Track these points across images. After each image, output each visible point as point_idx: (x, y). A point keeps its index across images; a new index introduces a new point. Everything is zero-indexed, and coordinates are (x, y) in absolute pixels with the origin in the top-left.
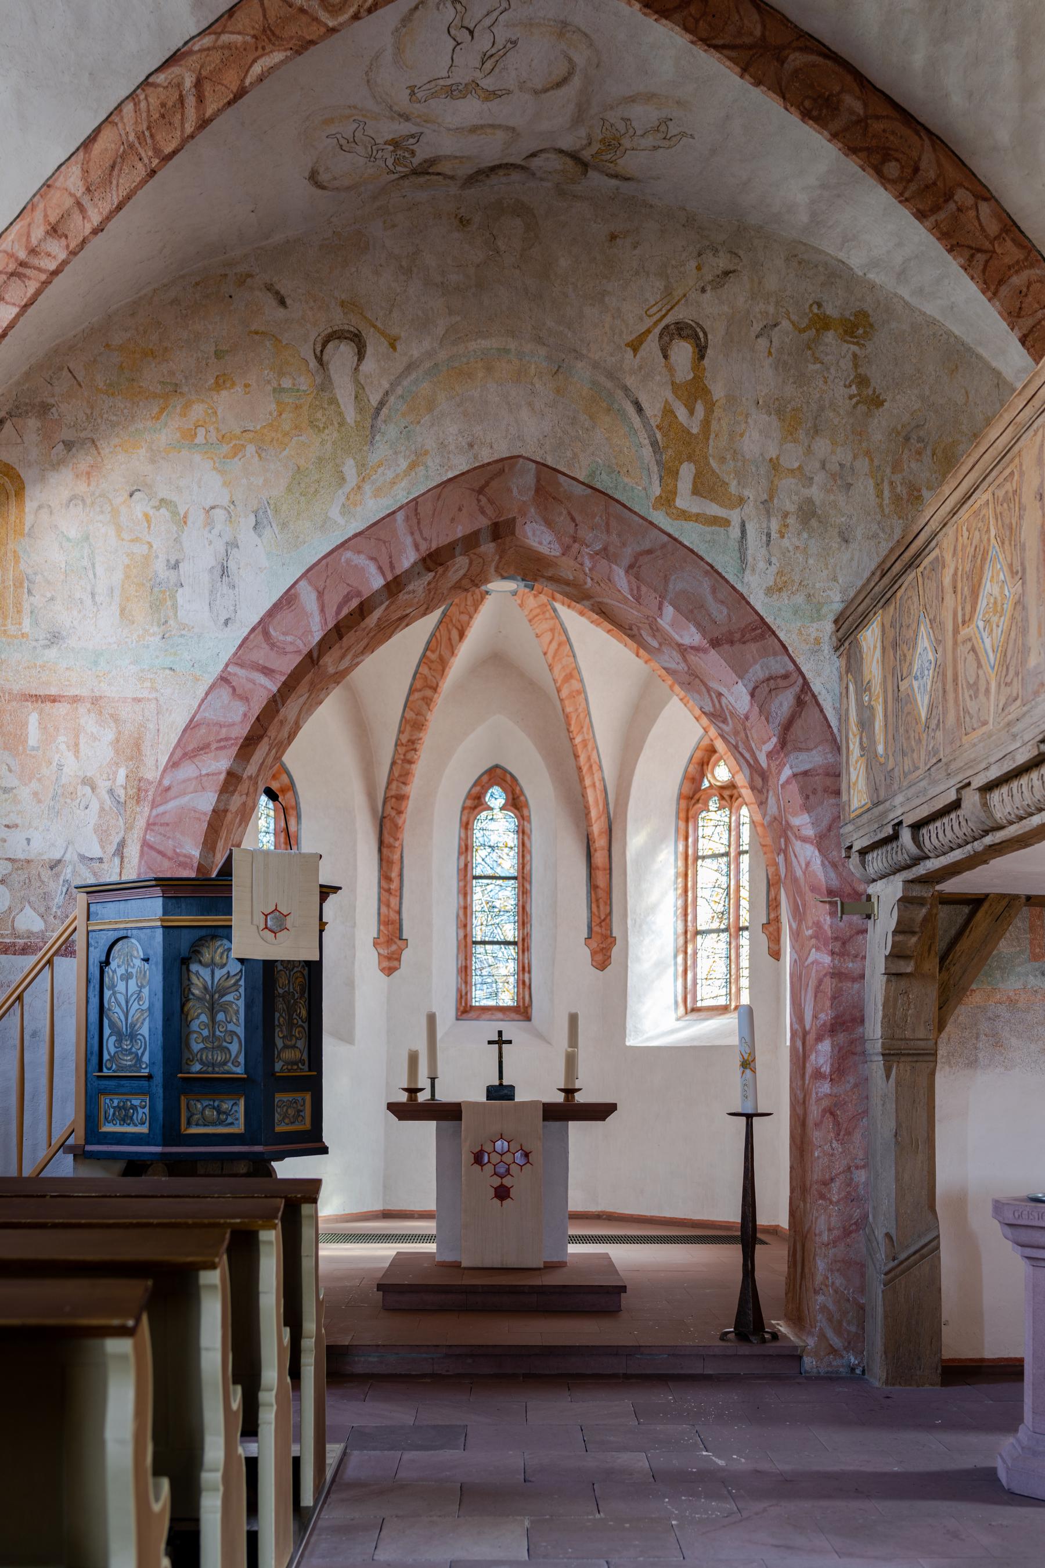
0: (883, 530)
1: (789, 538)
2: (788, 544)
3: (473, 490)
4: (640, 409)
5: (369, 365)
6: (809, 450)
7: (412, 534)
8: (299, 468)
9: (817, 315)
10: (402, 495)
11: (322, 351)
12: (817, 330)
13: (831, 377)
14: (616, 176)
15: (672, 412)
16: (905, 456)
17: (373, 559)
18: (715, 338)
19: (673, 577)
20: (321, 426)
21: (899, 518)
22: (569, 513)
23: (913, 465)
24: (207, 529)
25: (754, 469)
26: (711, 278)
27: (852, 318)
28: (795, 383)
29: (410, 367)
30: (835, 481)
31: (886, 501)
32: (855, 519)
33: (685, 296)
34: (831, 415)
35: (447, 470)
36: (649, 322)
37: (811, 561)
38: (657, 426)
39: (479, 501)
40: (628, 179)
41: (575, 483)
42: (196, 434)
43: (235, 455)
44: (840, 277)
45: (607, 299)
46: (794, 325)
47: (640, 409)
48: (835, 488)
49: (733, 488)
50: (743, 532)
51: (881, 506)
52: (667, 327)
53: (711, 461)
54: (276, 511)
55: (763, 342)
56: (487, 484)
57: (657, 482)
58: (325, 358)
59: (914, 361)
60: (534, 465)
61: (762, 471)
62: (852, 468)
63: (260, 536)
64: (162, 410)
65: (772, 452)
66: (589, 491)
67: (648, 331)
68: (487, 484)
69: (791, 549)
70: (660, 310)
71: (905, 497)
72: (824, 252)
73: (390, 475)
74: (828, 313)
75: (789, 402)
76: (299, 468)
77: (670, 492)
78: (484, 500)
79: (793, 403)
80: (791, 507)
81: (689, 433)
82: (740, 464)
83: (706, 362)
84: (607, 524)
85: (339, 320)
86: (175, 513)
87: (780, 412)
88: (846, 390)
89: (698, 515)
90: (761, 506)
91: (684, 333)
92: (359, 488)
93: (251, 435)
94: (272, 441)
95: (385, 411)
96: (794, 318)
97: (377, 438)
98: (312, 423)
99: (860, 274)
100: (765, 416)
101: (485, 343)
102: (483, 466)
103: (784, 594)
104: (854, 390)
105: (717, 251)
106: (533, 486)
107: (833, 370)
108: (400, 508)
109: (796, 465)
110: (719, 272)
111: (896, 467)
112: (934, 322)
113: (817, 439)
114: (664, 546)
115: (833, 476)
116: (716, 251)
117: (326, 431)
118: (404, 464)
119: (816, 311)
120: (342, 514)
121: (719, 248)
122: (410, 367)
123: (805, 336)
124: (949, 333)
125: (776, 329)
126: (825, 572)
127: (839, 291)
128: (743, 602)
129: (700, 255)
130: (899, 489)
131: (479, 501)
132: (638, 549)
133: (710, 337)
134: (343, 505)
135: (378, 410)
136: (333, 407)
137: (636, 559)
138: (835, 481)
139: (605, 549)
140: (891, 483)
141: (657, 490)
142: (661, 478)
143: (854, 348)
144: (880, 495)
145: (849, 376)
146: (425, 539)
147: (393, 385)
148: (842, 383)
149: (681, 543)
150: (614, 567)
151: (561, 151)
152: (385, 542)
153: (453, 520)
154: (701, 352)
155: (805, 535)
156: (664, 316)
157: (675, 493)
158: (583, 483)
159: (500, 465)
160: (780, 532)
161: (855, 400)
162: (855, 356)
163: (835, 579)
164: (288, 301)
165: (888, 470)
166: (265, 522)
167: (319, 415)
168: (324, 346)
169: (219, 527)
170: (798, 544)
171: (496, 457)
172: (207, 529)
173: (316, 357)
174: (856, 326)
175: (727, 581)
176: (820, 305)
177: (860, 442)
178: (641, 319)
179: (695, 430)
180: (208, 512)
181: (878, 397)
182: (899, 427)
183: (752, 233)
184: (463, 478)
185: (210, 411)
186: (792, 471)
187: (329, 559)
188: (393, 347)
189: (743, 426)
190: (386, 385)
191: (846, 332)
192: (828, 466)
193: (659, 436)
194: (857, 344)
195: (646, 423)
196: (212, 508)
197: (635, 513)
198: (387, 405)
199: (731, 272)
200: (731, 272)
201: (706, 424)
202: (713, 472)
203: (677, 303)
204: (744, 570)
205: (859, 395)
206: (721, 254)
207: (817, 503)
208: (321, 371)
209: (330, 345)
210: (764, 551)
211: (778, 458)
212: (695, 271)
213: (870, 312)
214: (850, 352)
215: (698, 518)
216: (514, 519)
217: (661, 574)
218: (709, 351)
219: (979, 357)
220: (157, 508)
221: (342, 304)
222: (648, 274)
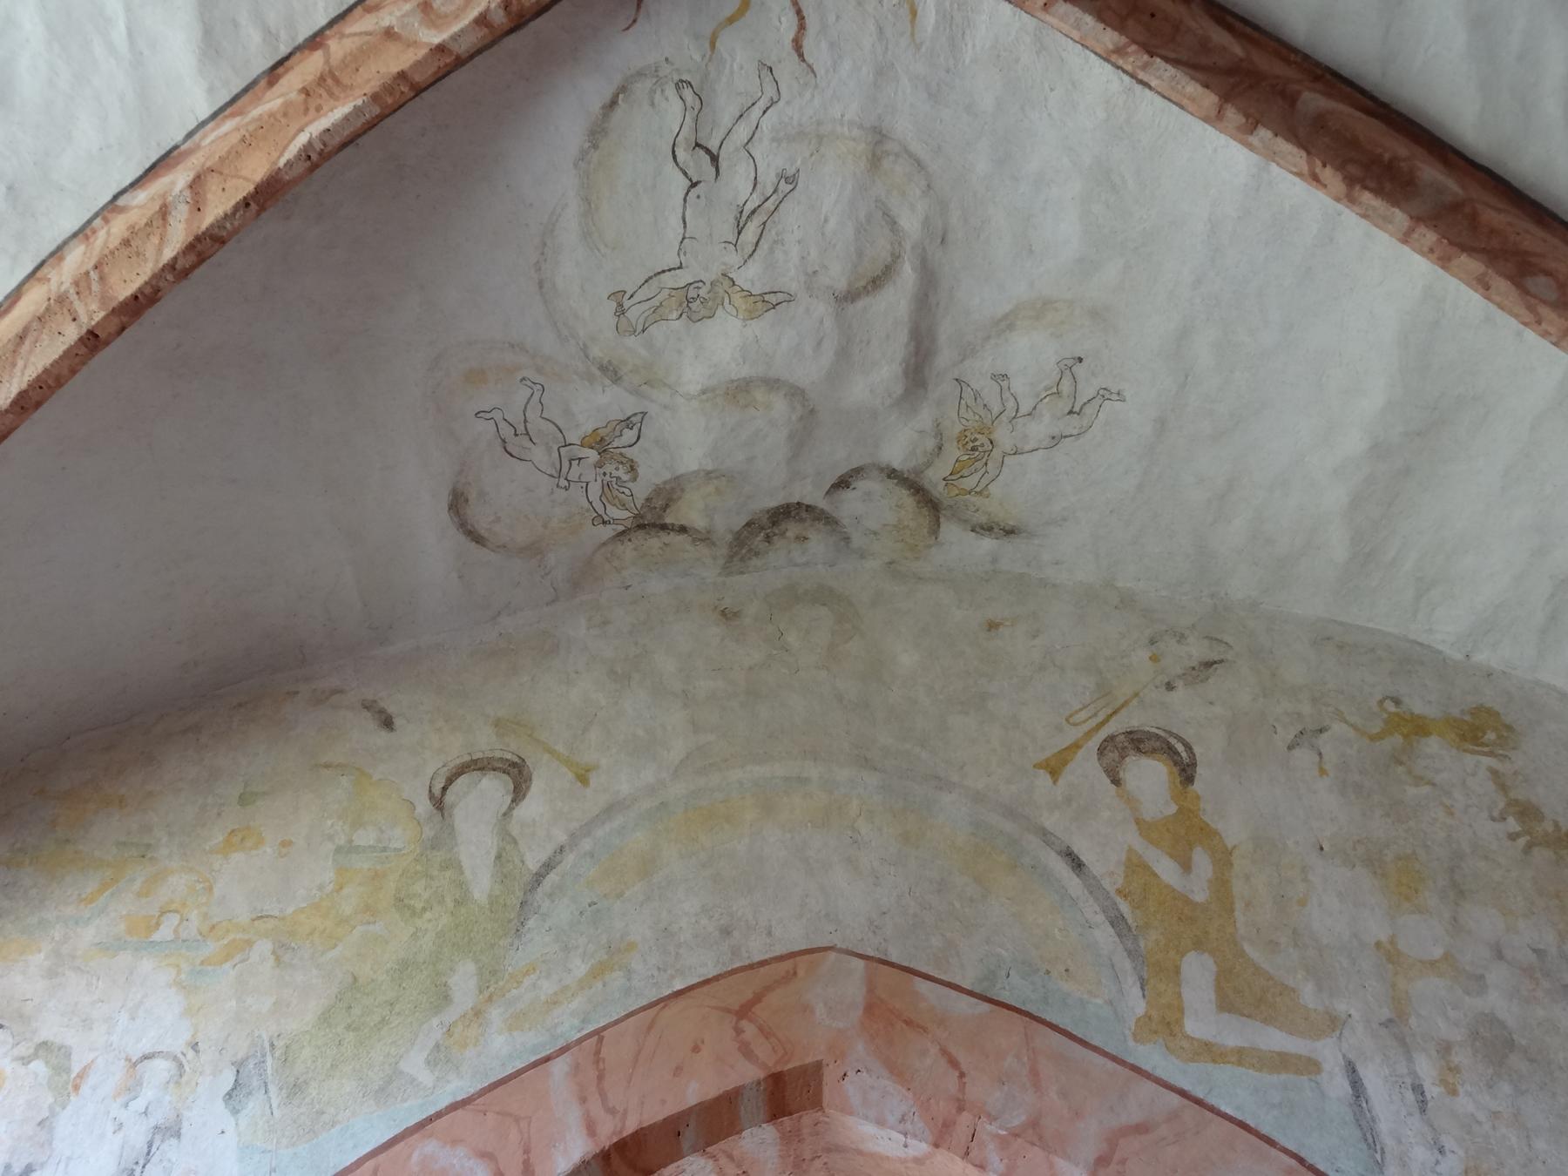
2: (1471, 1108)
3: (728, 1011)
4: (1077, 864)
5: (533, 806)
7: (583, 1100)
8: (355, 979)
10: (568, 1024)
11: (444, 789)
12: (1406, 736)
14: (987, 529)
15: (1146, 867)
17: (486, 1155)
18: (1209, 751)
20: (419, 905)
22: (944, 1052)
24: (121, 1100)
27: (1467, 718)
29: (609, 811)
35: (673, 977)
36: (1072, 735)
37: (1540, 1145)
39: (739, 1031)
40: (1010, 532)
42: (158, 925)
43: (227, 958)
47: (1077, 864)
49: (1308, 994)
50: (1356, 1084)
52: (1111, 739)
53: (1247, 948)
54: (286, 1061)
55: (1303, 756)
56: (758, 999)
57: (1136, 991)
58: (450, 798)
60: (859, 964)
63: (235, 1112)
64: (104, 887)
65: (1377, 930)
66: (985, 1007)
67: (1076, 746)
68: (758, 999)
69: (1481, 1116)
70: (1095, 715)
73: (548, 988)
76: (355, 979)
78: (750, 1029)
81: (1188, 902)
83: (1198, 786)
84: (1034, 1073)
85: (485, 742)
86: (60, 1069)
91: (1147, 746)
92: (477, 1013)
93: (270, 924)
94: (311, 934)
95: (553, 877)
97: (531, 923)
98: (400, 903)
99: (1459, 656)
102: (751, 967)
104: (1513, 824)
105: (1182, 636)
108: (564, 1050)
109: (1438, 953)
110: (1195, 664)
114: (1173, 1116)
116: (1181, 638)
117: (428, 915)
118: (580, 968)
120: (431, 1063)
122: (609, 811)
125: (1325, 736)
134: (437, 1046)
135: (539, 877)
136: (448, 874)
139: (1034, 1123)
141: (1140, 1007)
146: (612, 1111)
147: (574, 838)
150: (1060, 1163)
151: (892, 473)
152: (517, 1120)
153: (678, 1071)
154: (1186, 772)
156: (1103, 723)
157: (1181, 1010)
159: (788, 965)
160: (1444, 1082)
161: (1522, 841)
162: (1494, 773)
164: (398, 722)
166: (255, 1082)
167: (419, 887)
168: (450, 781)
169: (148, 1094)
171: (779, 950)
172: (121, 1100)
173: (431, 796)
179: (1200, 896)
180: (135, 1065)
184: (705, 989)
185: (199, 886)
186: (1433, 964)
187: (381, 1157)
188: (583, 779)
190: (561, 837)
193: (1124, 908)
194: (1491, 754)
195: (1093, 886)
196: (147, 1057)
197: (1095, 1049)
198: (559, 869)
200: (1215, 662)
201: (1221, 886)
203: (1123, 706)
208: (438, 817)
209: (462, 781)
211: (1392, 941)
215: (1241, 1057)
216: (818, 1067)
218: (1199, 770)
220: (25, 1061)
221: (497, 723)
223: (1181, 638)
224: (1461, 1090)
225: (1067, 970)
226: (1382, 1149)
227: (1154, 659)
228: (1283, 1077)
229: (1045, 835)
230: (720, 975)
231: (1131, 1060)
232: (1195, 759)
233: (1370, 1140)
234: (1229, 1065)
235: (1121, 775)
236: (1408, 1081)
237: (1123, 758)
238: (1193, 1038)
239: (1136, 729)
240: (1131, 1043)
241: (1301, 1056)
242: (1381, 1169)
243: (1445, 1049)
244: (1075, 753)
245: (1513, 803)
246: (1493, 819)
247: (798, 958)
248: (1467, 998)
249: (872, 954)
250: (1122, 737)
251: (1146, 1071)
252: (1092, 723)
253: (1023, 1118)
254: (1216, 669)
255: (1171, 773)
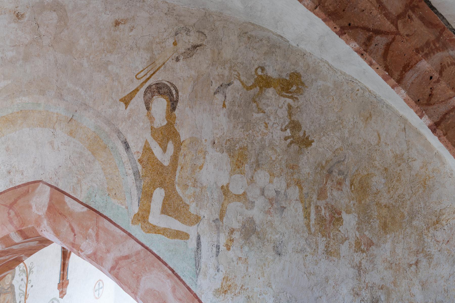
0: (309, 245)
1: (234, 250)
3: (6, 206)
4: (127, 147)
6: (252, 181)
9: (261, 76)
12: (261, 88)
13: (271, 123)
15: (150, 150)
16: (328, 186)
18: (183, 96)
19: (143, 278)
21: (323, 236)
22: (70, 226)
23: (335, 193)
25: (209, 194)
26: (183, 51)
27: (288, 78)
28: (243, 128)
30: (272, 205)
31: (313, 222)
32: (286, 236)
33: (164, 64)
34: (270, 152)
36: (137, 83)
37: (250, 270)
38: (139, 160)
39: (9, 214)
41: (76, 202)
44: (280, 47)
45: (110, 68)
46: (243, 84)
47: (127, 147)
48: (272, 210)
49: (193, 209)
51: (308, 225)
52: (150, 87)
53: (177, 188)
55: (219, 97)
56: (15, 202)
57: (137, 203)
59: (336, 110)
60: (48, 188)
61: (216, 196)
62: (285, 195)
66: (86, 209)
67: (137, 90)
68: (15, 202)
69: (235, 259)
70: (146, 74)
71: (328, 218)
72: (267, 30)
74: (269, 75)
75: (238, 142)
77: (145, 210)
78: (12, 213)
79: (240, 143)
80: (236, 225)
81: (162, 165)
82: (198, 190)
83: (176, 112)
84: (97, 235)
87: (230, 151)
88: (282, 133)
89: (165, 229)
90: (213, 224)
91: (162, 91)
96: (243, 78)
99: (294, 45)
100: (219, 153)
101: (26, 99)
102: (15, 188)
103: (229, 296)
104: (288, 133)
105: (189, 31)
106: (47, 204)
107: (272, 118)
109: (241, 192)
110: (190, 46)
111: (322, 194)
112: (353, 81)
113: (259, 171)
114: (138, 253)
115: (271, 201)
116: (188, 31)
119: (260, 73)
121: (191, 29)
123: (252, 92)
124: (365, 89)
125: (230, 87)
126: (262, 279)
127: (278, 58)
128: (196, 300)
129: (176, 34)
130: (323, 212)
131: (9, 214)
132: (119, 255)
133: (180, 94)
137: (117, 263)
138: (272, 205)
139: (95, 254)
140: (317, 207)
142: (140, 200)
143: (289, 101)
144: (307, 216)
145: (285, 122)
148: (279, 128)
149: (151, 251)
155: (246, 249)
156: (148, 79)
157: (149, 212)
158: (82, 203)
159: (25, 188)
161: (289, 141)
162: (290, 106)
163: (269, 285)
165: (315, 197)
170: (240, 256)
171: (25, 181)
174: (290, 84)
175: (184, 283)
176: (263, 69)
177: (292, 174)
178: (132, 81)
179: (166, 164)
181: (307, 138)
182: (324, 163)
183: (215, 17)
186: (238, 196)
189: (202, 160)
191: (283, 89)
192: (266, 193)
194: (291, 97)
199: (198, 46)
200: (198, 46)
201: (175, 158)
202: (178, 196)
203: (158, 69)
204: (197, 275)
205: (292, 136)
206: (191, 33)
207: (257, 222)
210: (214, 260)
211: (227, 186)
212: (172, 46)
213: (302, 74)
214: (286, 104)
215: (164, 232)
217: (134, 275)
218: (179, 104)
219: (388, 106)
222: (139, 49)
223: (188, 31)
224: (231, 248)
225: (115, 194)
226: (200, 269)
227: (175, 44)
228: (176, 240)
229: (118, 133)
230: (5, 191)
231: (129, 231)
232: (178, 99)
233: (197, 265)
234: (160, 234)
235: (150, 106)
236: (216, 244)
237: (152, 96)
238: (150, 224)
239: (160, 82)
240: (131, 224)
241: (184, 232)
242: (197, 276)
243: (232, 231)
244: (136, 93)
245: (292, 122)
246: (282, 130)
247: (30, 185)
248: (246, 210)
249: (53, 185)
250: (154, 86)
251: (133, 236)
252: (144, 79)
253: (92, 251)
254: (198, 49)
255: (168, 105)
